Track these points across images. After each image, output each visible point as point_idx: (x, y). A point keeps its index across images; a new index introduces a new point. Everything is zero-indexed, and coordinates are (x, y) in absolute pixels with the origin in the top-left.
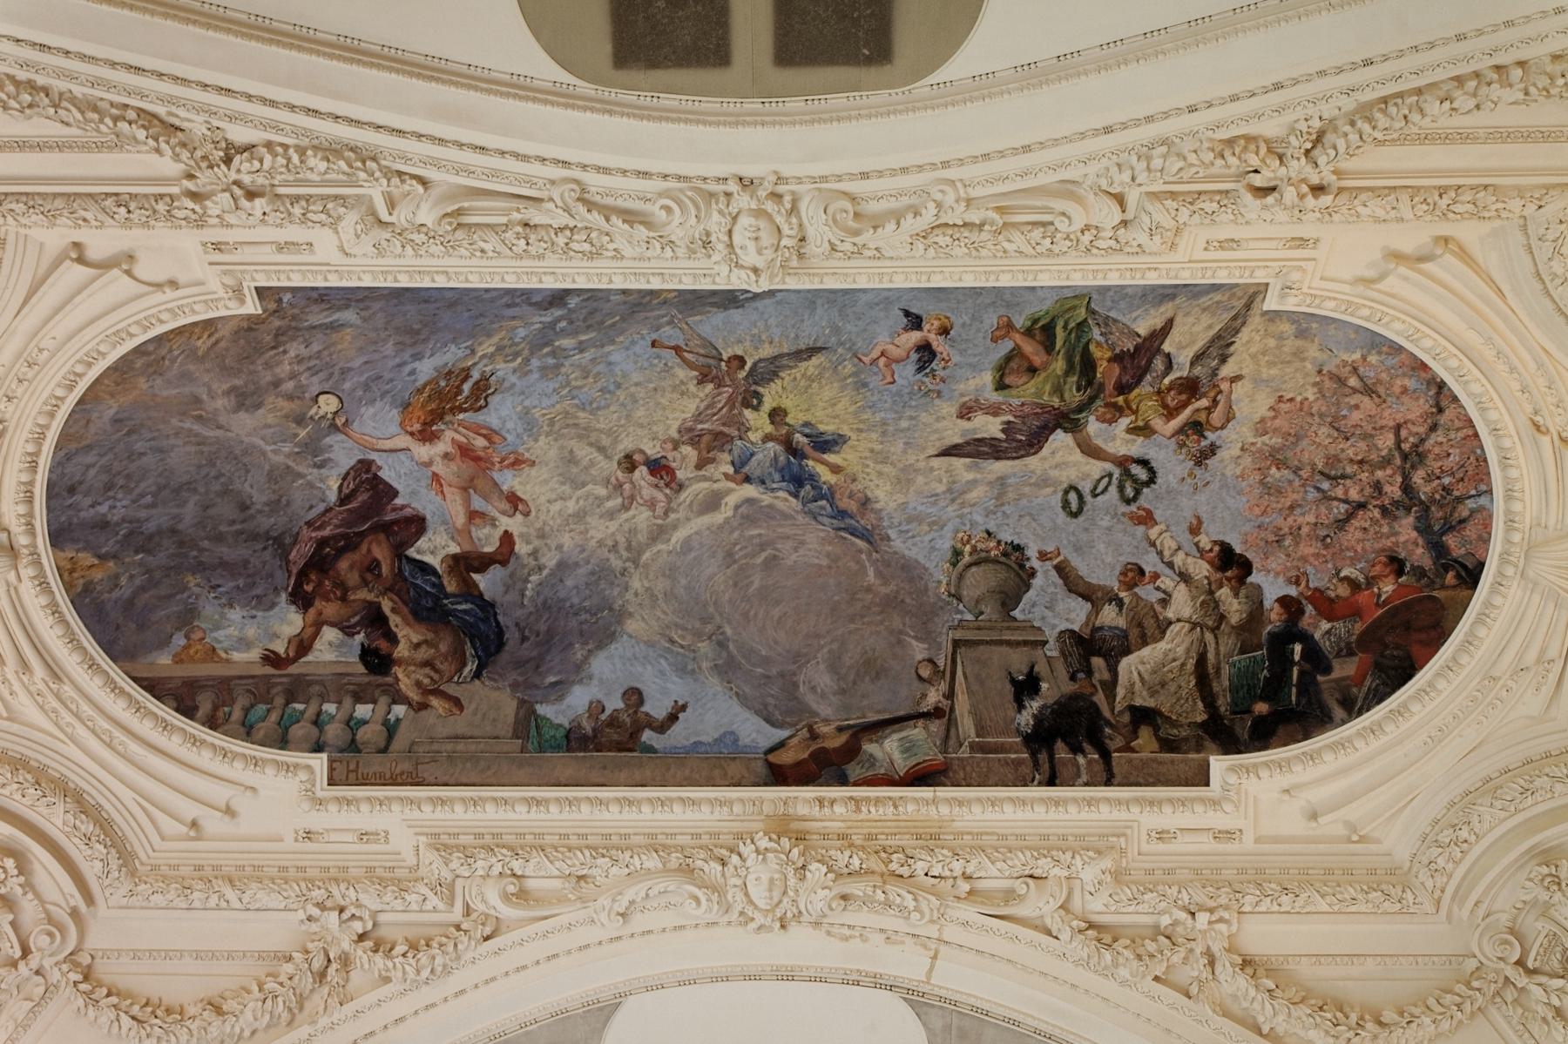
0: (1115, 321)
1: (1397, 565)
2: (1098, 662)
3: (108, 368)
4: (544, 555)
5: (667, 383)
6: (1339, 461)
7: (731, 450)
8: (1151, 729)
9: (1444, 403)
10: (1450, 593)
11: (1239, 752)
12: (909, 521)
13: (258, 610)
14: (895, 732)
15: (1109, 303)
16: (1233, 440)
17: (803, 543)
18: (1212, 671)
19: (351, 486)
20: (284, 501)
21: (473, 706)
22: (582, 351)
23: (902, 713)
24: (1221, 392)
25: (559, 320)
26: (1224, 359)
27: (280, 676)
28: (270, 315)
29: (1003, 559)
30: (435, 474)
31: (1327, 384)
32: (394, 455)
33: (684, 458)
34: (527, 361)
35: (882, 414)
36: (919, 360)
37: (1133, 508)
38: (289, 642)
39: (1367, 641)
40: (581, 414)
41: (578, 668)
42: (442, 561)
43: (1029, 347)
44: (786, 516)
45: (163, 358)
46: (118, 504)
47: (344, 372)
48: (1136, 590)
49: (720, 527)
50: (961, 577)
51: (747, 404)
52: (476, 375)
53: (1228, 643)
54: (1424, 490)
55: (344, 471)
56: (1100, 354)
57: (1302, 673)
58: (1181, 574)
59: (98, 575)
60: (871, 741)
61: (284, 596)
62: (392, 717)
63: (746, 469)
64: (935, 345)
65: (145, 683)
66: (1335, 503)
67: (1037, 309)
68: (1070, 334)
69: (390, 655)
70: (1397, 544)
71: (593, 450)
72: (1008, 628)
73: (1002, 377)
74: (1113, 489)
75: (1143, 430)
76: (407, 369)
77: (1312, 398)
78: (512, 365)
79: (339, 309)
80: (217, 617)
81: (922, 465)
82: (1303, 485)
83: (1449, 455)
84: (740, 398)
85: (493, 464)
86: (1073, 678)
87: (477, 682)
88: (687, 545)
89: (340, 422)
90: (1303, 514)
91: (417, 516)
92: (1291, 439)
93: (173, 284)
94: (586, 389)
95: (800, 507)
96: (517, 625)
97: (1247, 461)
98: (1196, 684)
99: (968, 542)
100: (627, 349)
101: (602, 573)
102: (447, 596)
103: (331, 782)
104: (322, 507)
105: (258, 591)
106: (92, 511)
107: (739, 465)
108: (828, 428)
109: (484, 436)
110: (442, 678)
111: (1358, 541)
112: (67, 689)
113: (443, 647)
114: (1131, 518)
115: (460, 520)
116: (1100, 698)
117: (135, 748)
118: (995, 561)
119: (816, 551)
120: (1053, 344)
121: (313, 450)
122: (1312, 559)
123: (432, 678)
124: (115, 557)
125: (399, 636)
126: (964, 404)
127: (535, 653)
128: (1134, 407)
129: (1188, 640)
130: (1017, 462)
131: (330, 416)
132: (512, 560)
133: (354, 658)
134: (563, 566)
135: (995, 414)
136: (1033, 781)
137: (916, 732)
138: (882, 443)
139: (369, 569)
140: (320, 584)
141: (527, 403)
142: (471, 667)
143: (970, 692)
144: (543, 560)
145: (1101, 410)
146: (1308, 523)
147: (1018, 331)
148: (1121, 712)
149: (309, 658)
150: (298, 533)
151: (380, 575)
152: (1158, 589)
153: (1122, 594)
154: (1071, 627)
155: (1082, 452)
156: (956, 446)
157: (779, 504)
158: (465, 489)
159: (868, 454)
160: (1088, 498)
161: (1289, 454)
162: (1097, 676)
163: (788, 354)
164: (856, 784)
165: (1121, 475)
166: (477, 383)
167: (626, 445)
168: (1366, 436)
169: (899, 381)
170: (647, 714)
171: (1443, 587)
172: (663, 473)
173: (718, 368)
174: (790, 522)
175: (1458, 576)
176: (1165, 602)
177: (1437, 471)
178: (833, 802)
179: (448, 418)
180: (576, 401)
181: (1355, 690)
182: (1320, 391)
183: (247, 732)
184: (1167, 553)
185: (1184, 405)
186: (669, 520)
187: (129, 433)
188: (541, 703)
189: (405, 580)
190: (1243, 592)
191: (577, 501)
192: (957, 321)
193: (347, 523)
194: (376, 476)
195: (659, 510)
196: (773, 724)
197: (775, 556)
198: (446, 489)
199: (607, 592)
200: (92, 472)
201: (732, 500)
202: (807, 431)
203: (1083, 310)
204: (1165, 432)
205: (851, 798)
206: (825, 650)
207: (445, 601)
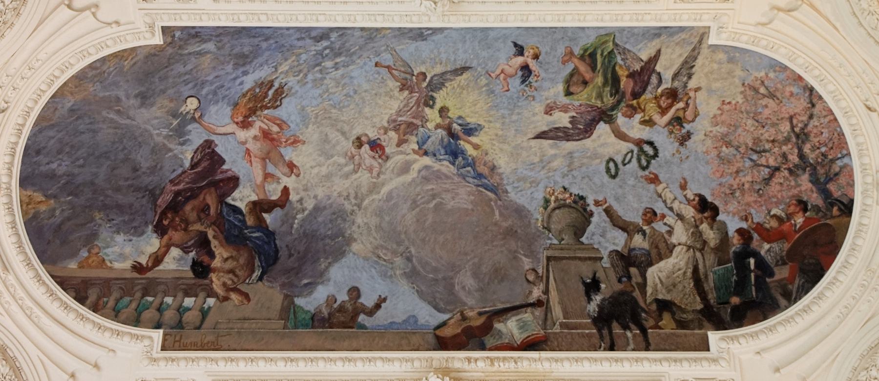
0: (629, 51)
1: (803, 205)
2: (633, 270)
3: (73, 76)
4: (306, 202)
5: (382, 90)
6: (761, 141)
7: (417, 134)
8: (670, 314)
9: (815, 101)
10: (837, 220)
11: (726, 329)
12: (519, 180)
13: (134, 236)
14: (514, 315)
15: (625, 39)
16: (701, 128)
17: (457, 194)
18: (702, 277)
19: (199, 157)
20: (159, 167)
21: (256, 299)
22: (337, 69)
23: (517, 303)
24: (690, 98)
25: (325, 48)
26: (690, 77)
27: (141, 279)
28: (168, 45)
29: (573, 205)
30: (247, 149)
31: (748, 92)
32: (224, 137)
33: (390, 139)
34: (306, 75)
35: (502, 111)
36: (522, 76)
37: (647, 173)
38: (149, 257)
39: (791, 256)
40: (333, 111)
41: (322, 274)
42: (246, 205)
43: (583, 68)
44: (447, 177)
45: (104, 72)
46: (63, 164)
47: (203, 83)
48: (653, 225)
49: (410, 184)
50: (550, 217)
51: (427, 104)
52: (276, 85)
53: (711, 258)
54: (812, 157)
55: (195, 147)
56: (622, 73)
57: (756, 277)
58: (678, 215)
59: (43, 208)
60: (499, 322)
61: (150, 227)
62: (206, 306)
63: (425, 147)
64: (531, 65)
65: (58, 280)
66: (762, 168)
67: (586, 43)
68: (605, 59)
69: (209, 265)
70: (801, 192)
71: (338, 134)
72: (579, 249)
73: (568, 87)
74: (634, 160)
75: (648, 122)
76: (238, 81)
77: (741, 101)
78: (297, 78)
79: (204, 41)
80: (109, 239)
81: (525, 144)
82: (742, 158)
83: (822, 133)
84: (423, 101)
85: (281, 143)
86: (620, 281)
87: (260, 283)
88: (389, 196)
89: (197, 115)
90: (744, 176)
91: (234, 176)
92: (732, 128)
93: (117, 23)
94: (337, 94)
95: (455, 171)
96: (287, 246)
97: (709, 142)
98: (695, 285)
99: (553, 194)
100: (362, 68)
101: (340, 215)
102: (247, 228)
103: (164, 348)
104: (180, 171)
105: (135, 224)
106: (47, 167)
107: (421, 144)
108: (472, 120)
109: (278, 125)
110: (239, 280)
111: (779, 191)
112: (11, 279)
113: (242, 261)
114: (646, 179)
115: (259, 179)
116: (637, 294)
117: (45, 321)
118: (569, 206)
119: (465, 200)
120: (596, 65)
121: (180, 133)
122: (753, 204)
123: (233, 281)
124: (55, 197)
125: (216, 253)
126: (548, 105)
127: (296, 265)
128: (643, 107)
129: (686, 257)
130: (579, 142)
131: (192, 112)
132: (288, 205)
133: (187, 268)
134: (317, 209)
135: (566, 112)
136: (600, 348)
137: (527, 315)
138: (502, 130)
139: (203, 211)
140: (173, 220)
141: (304, 103)
142: (257, 273)
143: (559, 291)
144: (305, 205)
145: (625, 109)
146: (748, 182)
147: (576, 57)
148: (651, 303)
149: (161, 267)
150: (164, 188)
151: (209, 214)
152: (665, 224)
153: (645, 228)
154: (616, 248)
155: (616, 136)
156: (544, 132)
157: (444, 170)
158: (264, 159)
159: (494, 137)
160: (620, 166)
161: (732, 138)
162: (634, 280)
163: (451, 72)
164: (490, 349)
165: (638, 151)
166: (276, 90)
167: (357, 131)
168: (774, 125)
169: (511, 89)
170: (362, 304)
171: (832, 217)
172: (378, 149)
173: (411, 80)
174: (450, 181)
175: (840, 209)
176: (670, 233)
177: (817, 144)
178: (476, 360)
179: (258, 113)
180: (331, 102)
181: (790, 287)
182: (745, 97)
183: (116, 315)
184: (668, 202)
185: (670, 106)
186: (380, 180)
187: (78, 118)
188: (298, 296)
189: (224, 217)
190: (715, 226)
191: (328, 167)
192: (543, 50)
193: (194, 181)
194: (214, 151)
195: (375, 173)
196: (439, 310)
197: (441, 203)
198: (253, 159)
199: (342, 226)
200: (52, 142)
201: (416, 167)
202: (460, 122)
203: (611, 43)
204: (661, 124)
205: (488, 358)
206: (470, 263)
207: (246, 231)
